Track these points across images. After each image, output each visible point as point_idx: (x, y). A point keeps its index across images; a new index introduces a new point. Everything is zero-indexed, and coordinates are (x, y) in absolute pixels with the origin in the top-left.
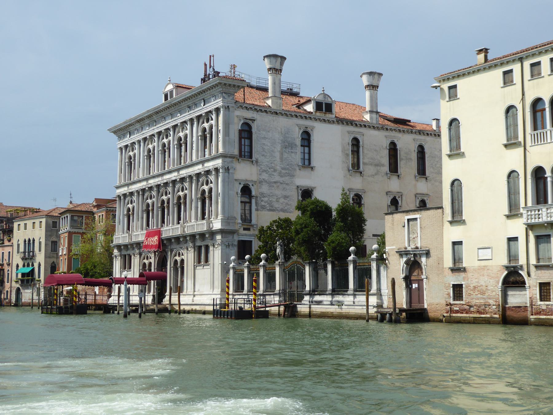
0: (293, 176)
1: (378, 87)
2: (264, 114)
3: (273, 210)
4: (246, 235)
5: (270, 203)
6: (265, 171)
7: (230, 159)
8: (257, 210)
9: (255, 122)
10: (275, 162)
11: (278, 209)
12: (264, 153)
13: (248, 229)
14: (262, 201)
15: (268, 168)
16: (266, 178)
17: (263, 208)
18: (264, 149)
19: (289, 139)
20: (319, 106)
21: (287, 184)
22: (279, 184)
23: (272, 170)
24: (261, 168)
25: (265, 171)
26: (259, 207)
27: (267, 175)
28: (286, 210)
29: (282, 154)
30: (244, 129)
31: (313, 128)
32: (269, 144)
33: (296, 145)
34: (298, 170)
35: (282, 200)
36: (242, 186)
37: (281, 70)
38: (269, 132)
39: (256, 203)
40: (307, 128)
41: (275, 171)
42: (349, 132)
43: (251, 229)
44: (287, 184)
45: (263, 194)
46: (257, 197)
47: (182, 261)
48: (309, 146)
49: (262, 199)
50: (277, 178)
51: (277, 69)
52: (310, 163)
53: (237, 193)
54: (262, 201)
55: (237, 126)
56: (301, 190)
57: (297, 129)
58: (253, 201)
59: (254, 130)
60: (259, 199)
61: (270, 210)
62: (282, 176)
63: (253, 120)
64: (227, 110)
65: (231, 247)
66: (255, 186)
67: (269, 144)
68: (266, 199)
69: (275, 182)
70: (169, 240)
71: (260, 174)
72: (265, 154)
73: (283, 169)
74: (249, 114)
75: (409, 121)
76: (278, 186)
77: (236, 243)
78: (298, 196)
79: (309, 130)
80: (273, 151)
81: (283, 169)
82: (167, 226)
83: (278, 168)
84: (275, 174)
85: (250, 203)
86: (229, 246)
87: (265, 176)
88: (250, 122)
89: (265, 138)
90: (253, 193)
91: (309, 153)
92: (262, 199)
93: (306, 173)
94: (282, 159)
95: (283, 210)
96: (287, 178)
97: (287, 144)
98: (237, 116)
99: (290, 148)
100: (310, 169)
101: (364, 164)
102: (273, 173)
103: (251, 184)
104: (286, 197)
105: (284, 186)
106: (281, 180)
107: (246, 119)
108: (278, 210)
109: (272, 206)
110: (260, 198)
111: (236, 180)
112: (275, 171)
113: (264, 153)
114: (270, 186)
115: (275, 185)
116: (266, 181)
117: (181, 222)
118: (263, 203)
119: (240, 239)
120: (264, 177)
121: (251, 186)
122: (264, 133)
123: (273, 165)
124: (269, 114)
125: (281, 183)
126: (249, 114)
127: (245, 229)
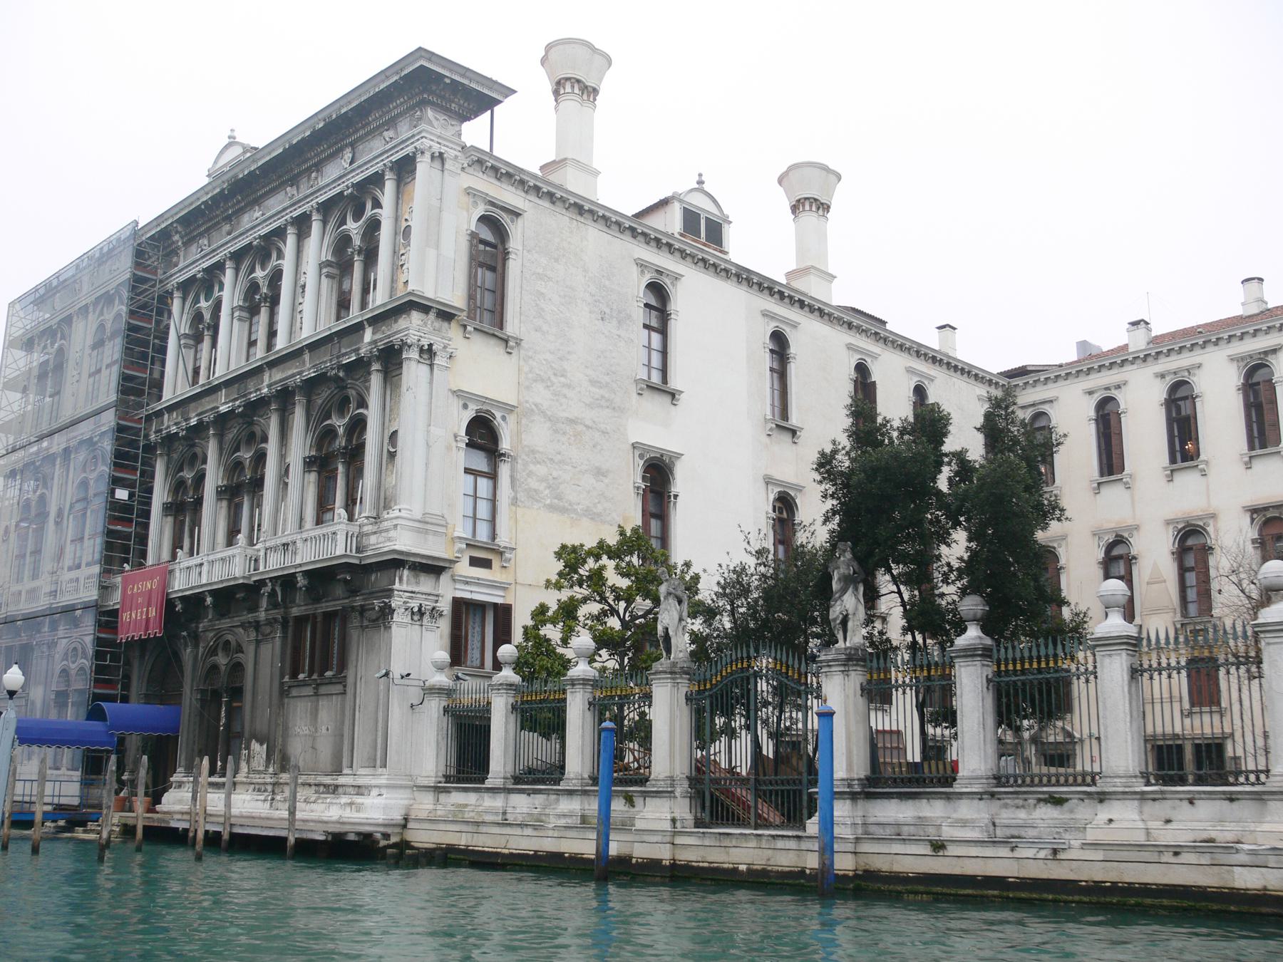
1: (829, 207)
2: (546, 204)
3: (563, 510)
4: (478, 582)
8: (514, 502)
9: (520, 220)
13: (486, 564)
17: (533, 495)
20: (691, 218)
22: (580, 428)
23: (562, 379)
26: (521, 496)
28: (599, 515)
30: (483, 236)
31: (677, 278)
33: (629, 317)
34: (635, 395)
36: (469, 415)
37: (595, 91)
38: (557, 260)
40: (660, 272)
42: (766, 314)
43: (496, 564)
45: (533, 452)
47: (237, 668)
48: (663, 331)
49: (532, 467)
51: (586, 87)
52: (665, 379)
53: (456, 436)
54: (530, 474)
55: (460, 223)
56: (641, 456)
57: (635, 270)
58: (504, 470)
59: (514, 244)
60: (519, 467)
61: (552, 508)
63: (516, 214)
64: (437, 164)
65: (426, 618)
66: (511, 419)
68: (541, 470)
69: (572, 421)
70: (194, 602)
72: (545, 328)
74: (509, 196)
75: (884, 323)
77: (445, 606)
79: (667, 282)
81: (593, 382)
82: (191, 554)
85: (493, 476)
86: (421, 613)
88: (505, 219)
90: (505, 445)
91: (664, 353)
92: (532, 467)
93: (656, 403)
98: (470, 192)
99: (614, 322)
100: (667, 399)
102: (565, 391)
103: (498, 415)
104: (599, 473)
107: (492, 204)
109: (559, 497)
114: (556, 431)
117: (241, 538)
118: (533, 484)
119: (459, 594)
121: (498, 421)
124: (559, 208)
126: (509, 196)
127: (474, 562)
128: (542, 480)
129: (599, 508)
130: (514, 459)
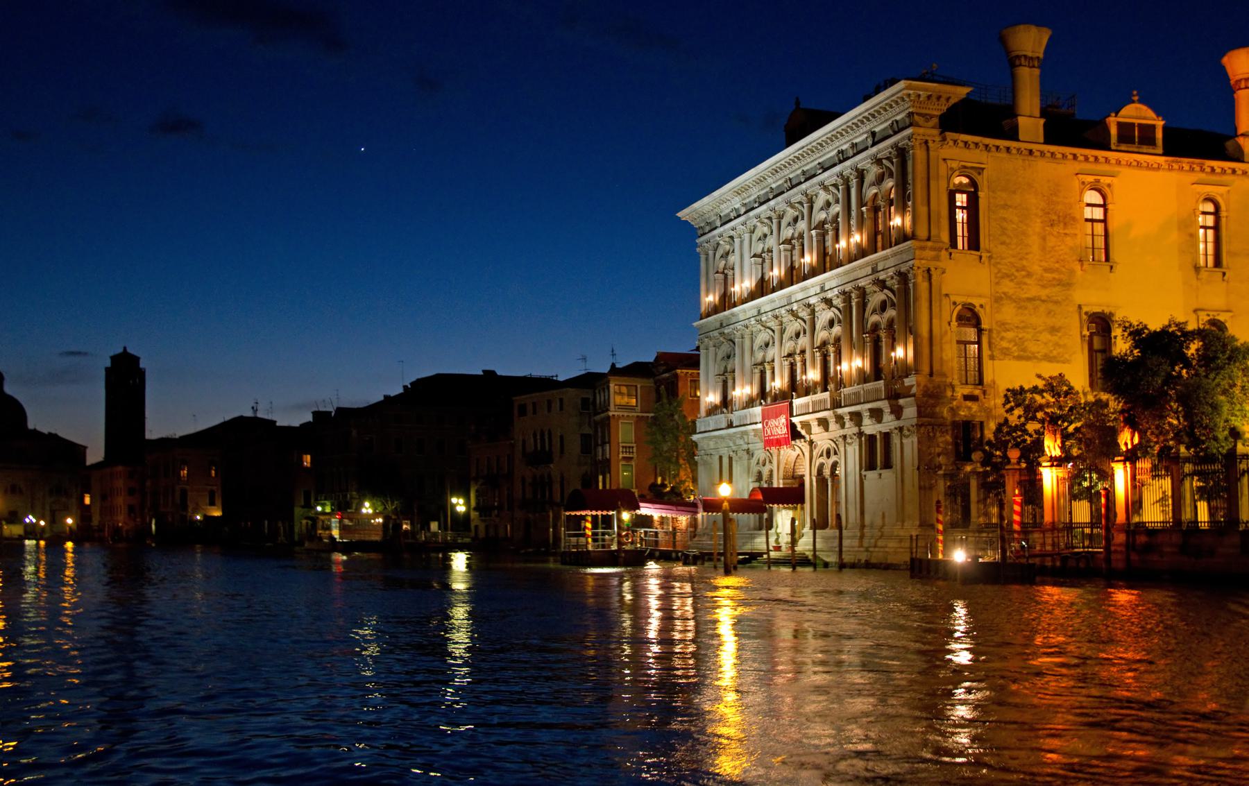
0: (1067, 285)
3: (1028, 359)
5: (1020, 343)
6: (1007, 276)
7: (933, 253)
10: (1030, 256)
11: (1039, 356)
12: (1004, 238)
14: (1002, 339)
15: (1013, 270)
16: (1011, 292)
17: (1006, 353)
18: (1004, 229)
19: (1059, 207)
21: (1056, 302)
24: (999, 271)
25: (1007, 276)
27: (1012, 284)
29: (1044, 239)
32: (1016, 219)
35: (1045, 336)
38: (1014, 192)
39: (990, 344)
41: (1029, 275)
44: (1056, 302)
46: (990, 331)
49: (1004, 334)
50: (1033, 290)
54: (1002, 339)
60: (994, 335)
61: (1019, 358)
62: (1044, 287)
67: (1016, 219)
68: (1010, 335)
69: (1029, 300)
71: (997, 283)
73: (1046, 270)
76: (1036, 308)
78: (1082, 327)
80: (1024, 233)
81: (1046, 270)
83: (1036, 268)
84: (1028, 281)
87: (1008, 287)
89: (1005, 206)
92: (1004, 334)
94: (1043, 249)
95: (1049, 358)
96: (1057, 289)
97: (1055, 218)
99: (1062, 225)
101: (1232, 254)
103: (977, 305)
105: (1051, 306)
106: (1044, 293)
108: (1036, 358)
109: (1024, 350)
110: (999, 333)
111: (947, 295)
112: (1029, 275)
113: (1004, 238)
114: (1020, 308)
115: (1029, 305)
116: (1010, 298)
118: (1005, 344)
120: (1006, 290)
122: (1004, 195)
123: (1025, 263)
125: (1043, 301)
128: (1010, 342)
129: (1055, 353)
130: (990, 331)
